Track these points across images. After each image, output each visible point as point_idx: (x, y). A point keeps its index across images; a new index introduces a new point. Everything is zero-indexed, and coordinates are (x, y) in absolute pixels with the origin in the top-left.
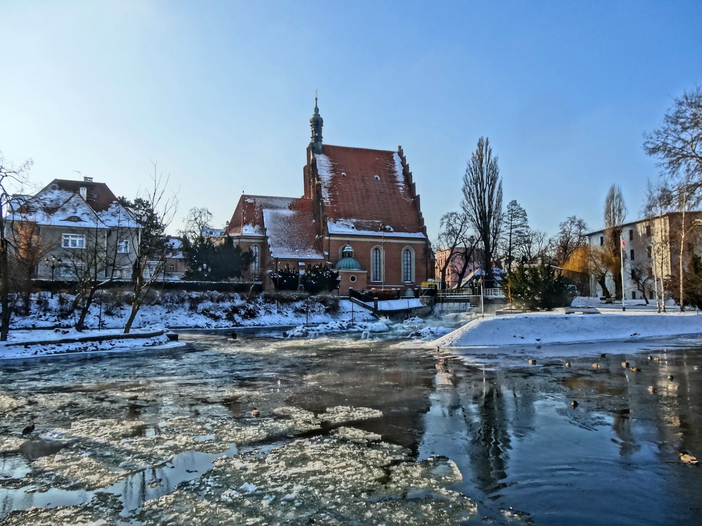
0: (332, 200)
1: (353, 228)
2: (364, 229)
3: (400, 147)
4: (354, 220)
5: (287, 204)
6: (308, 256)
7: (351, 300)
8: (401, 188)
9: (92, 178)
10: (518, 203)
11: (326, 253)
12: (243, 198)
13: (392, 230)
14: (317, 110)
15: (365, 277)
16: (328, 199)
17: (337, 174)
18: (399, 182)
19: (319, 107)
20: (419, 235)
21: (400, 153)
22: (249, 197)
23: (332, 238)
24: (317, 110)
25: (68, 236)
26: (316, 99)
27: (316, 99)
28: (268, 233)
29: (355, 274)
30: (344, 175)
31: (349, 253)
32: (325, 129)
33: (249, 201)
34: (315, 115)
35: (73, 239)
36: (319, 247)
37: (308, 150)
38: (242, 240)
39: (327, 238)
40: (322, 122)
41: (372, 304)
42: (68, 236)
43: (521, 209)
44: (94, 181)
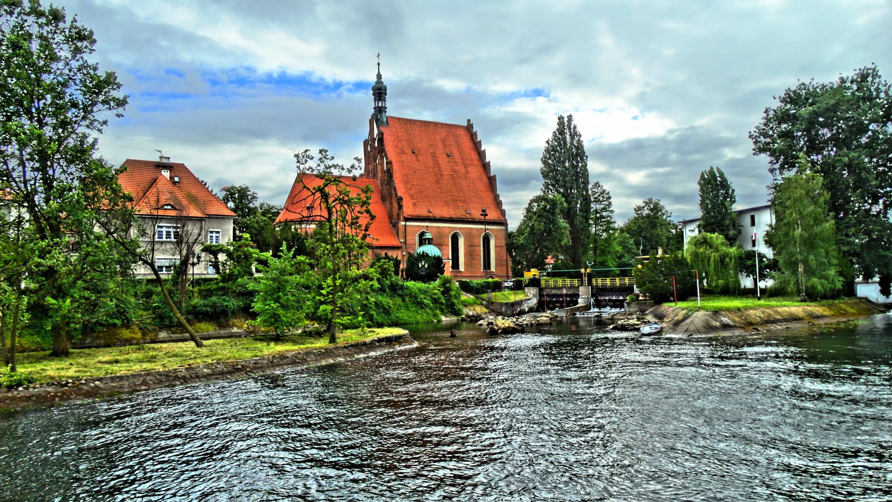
3: (469, 121)
9: (169, 158)
10: (601, 184)
14: (379, 76)
19: (381, 73)
21: (469, 128)
24: (379, 76)
25: (162, 227)
27: (379, 64)
31: (429, 239)
34: (377, 83)
35: (167, 230)
39: (403, 223)
42: (162, 227)
43: (604, 191)
44: (172, 161)
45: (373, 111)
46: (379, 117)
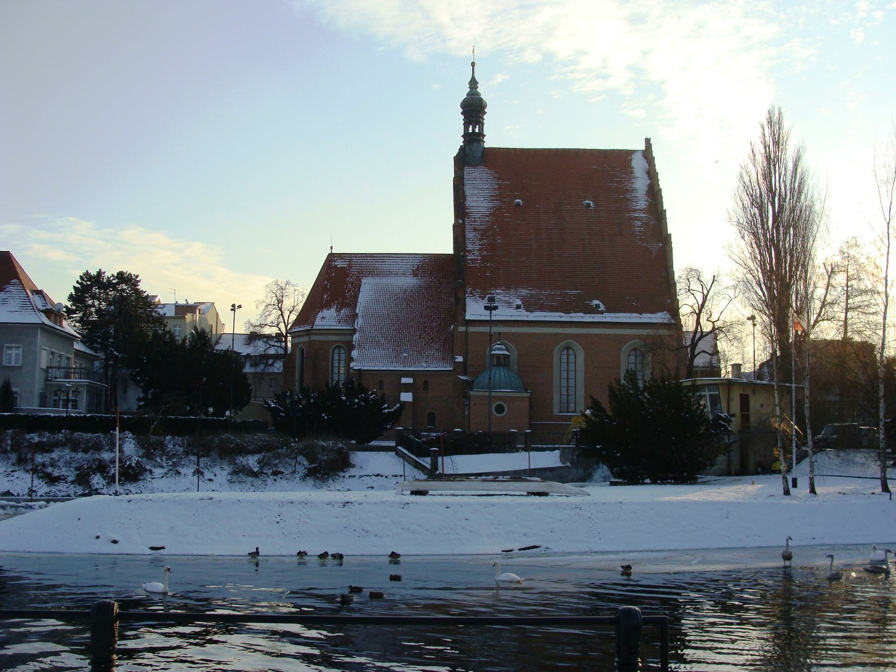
0: (485, 253)
1: (518, 307)
2: (542, 308)
3: (648, 141)
4: (524, 292)
5: (409, 266)
6: (423, 367)
7: (399, 454)
8: (639, 223)
11: (460, 359)
12: (331, 257)
13: (602, 307)
14: (473, 83)
15: (525, 405)
16: (476, 253)
17: (503, 202)
18: (635, 211)
20: (659, 317)
22: (341, 256)
23: (472, 329)
24: (473, 83)
26: (473, 64)
27: (473, 64)
28: (359, 322)
29: (505, 399)
30: (518, 205)
32: (487, 119)
33: (340, 264)
36: (448, 347)
37: (457, 159)
38: (314, 338)
39: (461, 329)
40: (485, 107)
41: (426, 462)
45: (460, 142)
46: (467, 150)
